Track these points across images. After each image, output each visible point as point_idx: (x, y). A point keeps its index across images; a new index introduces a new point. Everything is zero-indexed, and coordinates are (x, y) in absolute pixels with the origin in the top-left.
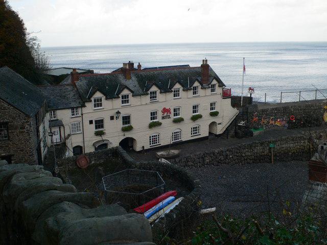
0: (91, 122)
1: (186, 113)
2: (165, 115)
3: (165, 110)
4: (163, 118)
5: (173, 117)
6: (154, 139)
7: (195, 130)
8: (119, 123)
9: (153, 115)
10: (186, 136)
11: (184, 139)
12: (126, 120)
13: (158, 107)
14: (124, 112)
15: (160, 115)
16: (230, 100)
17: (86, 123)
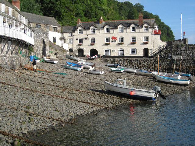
0: (77, 39)
1: (128, 40)
2: (113, 40)
3: (113, 38)
4: (112, 42)
5: (118, 41)
6: (108, 51)
7: (135, 51)
8: (90, 42)
9: (108, 40)
10: (128, 53)
11: (125, 55)
12: (93, 40)
13: (110, 36)
14: (94, 36)
15: (111, 40)
16: (159, 36)
17: (75, 39)
